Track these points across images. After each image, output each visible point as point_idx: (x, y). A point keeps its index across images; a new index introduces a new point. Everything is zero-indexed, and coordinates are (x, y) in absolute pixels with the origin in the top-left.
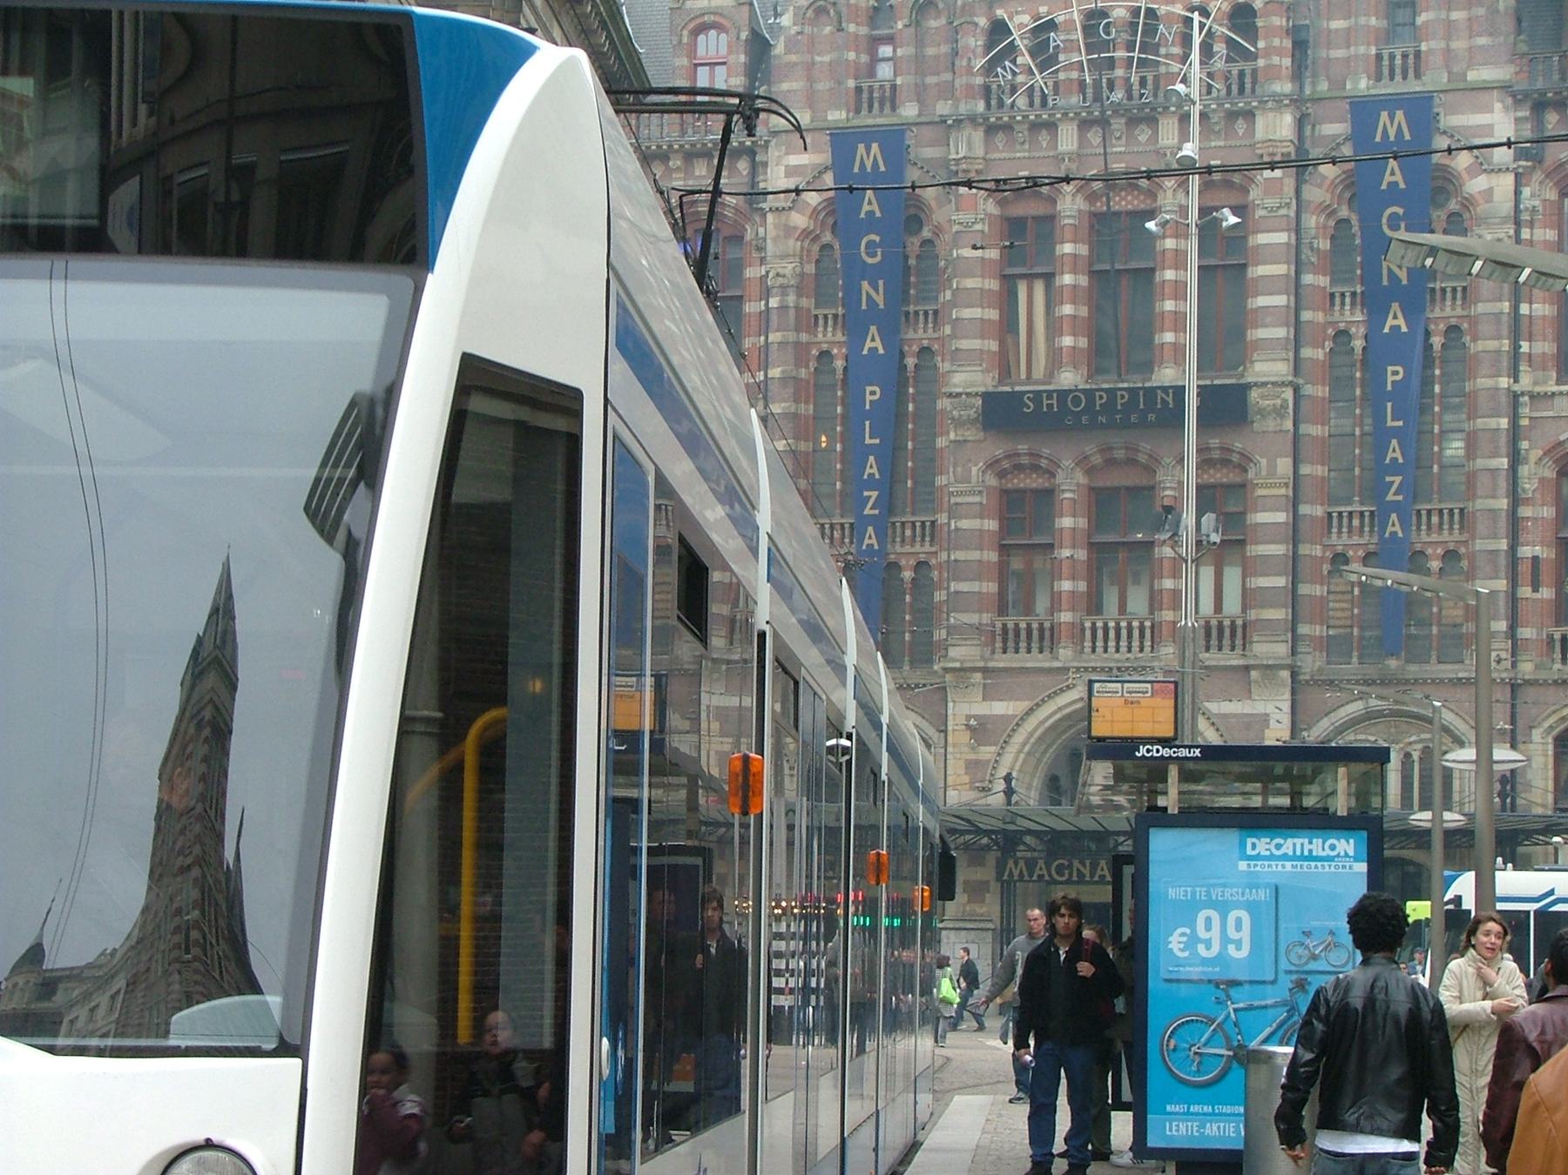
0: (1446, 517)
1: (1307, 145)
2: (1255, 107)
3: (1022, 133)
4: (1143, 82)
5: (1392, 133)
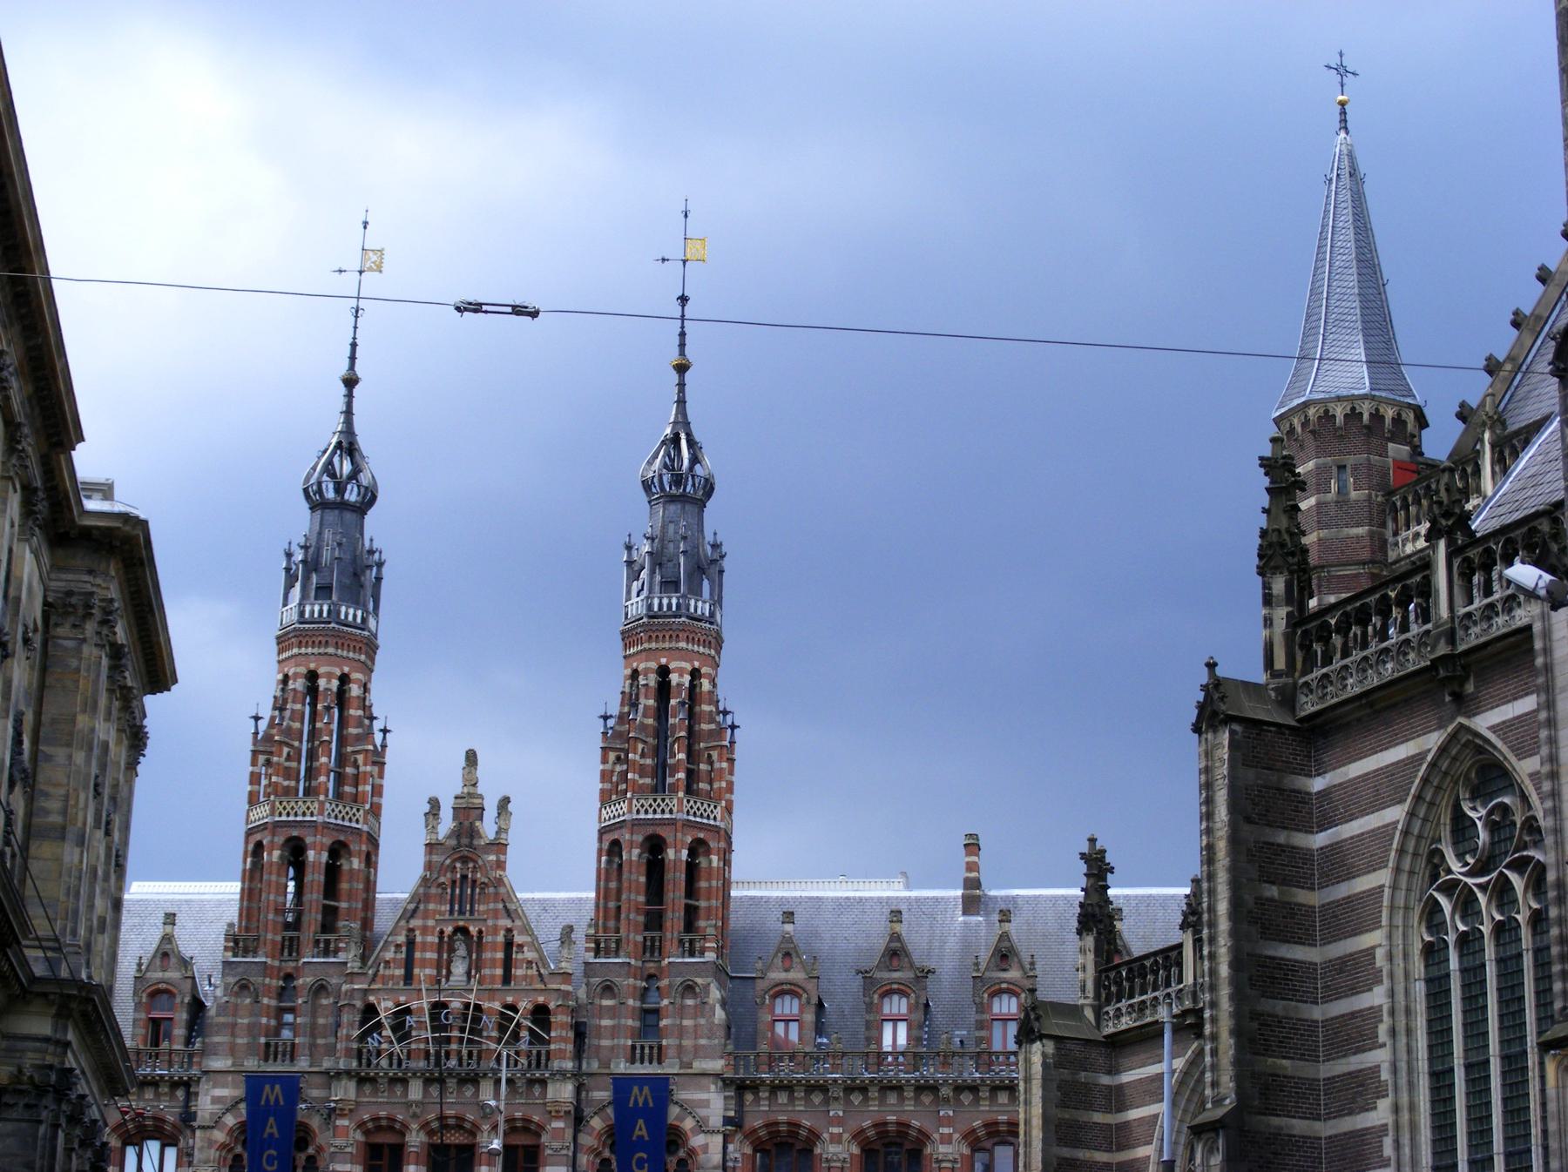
1: (583, 1105)
4: (470, 1054)
5: (641, 1101)
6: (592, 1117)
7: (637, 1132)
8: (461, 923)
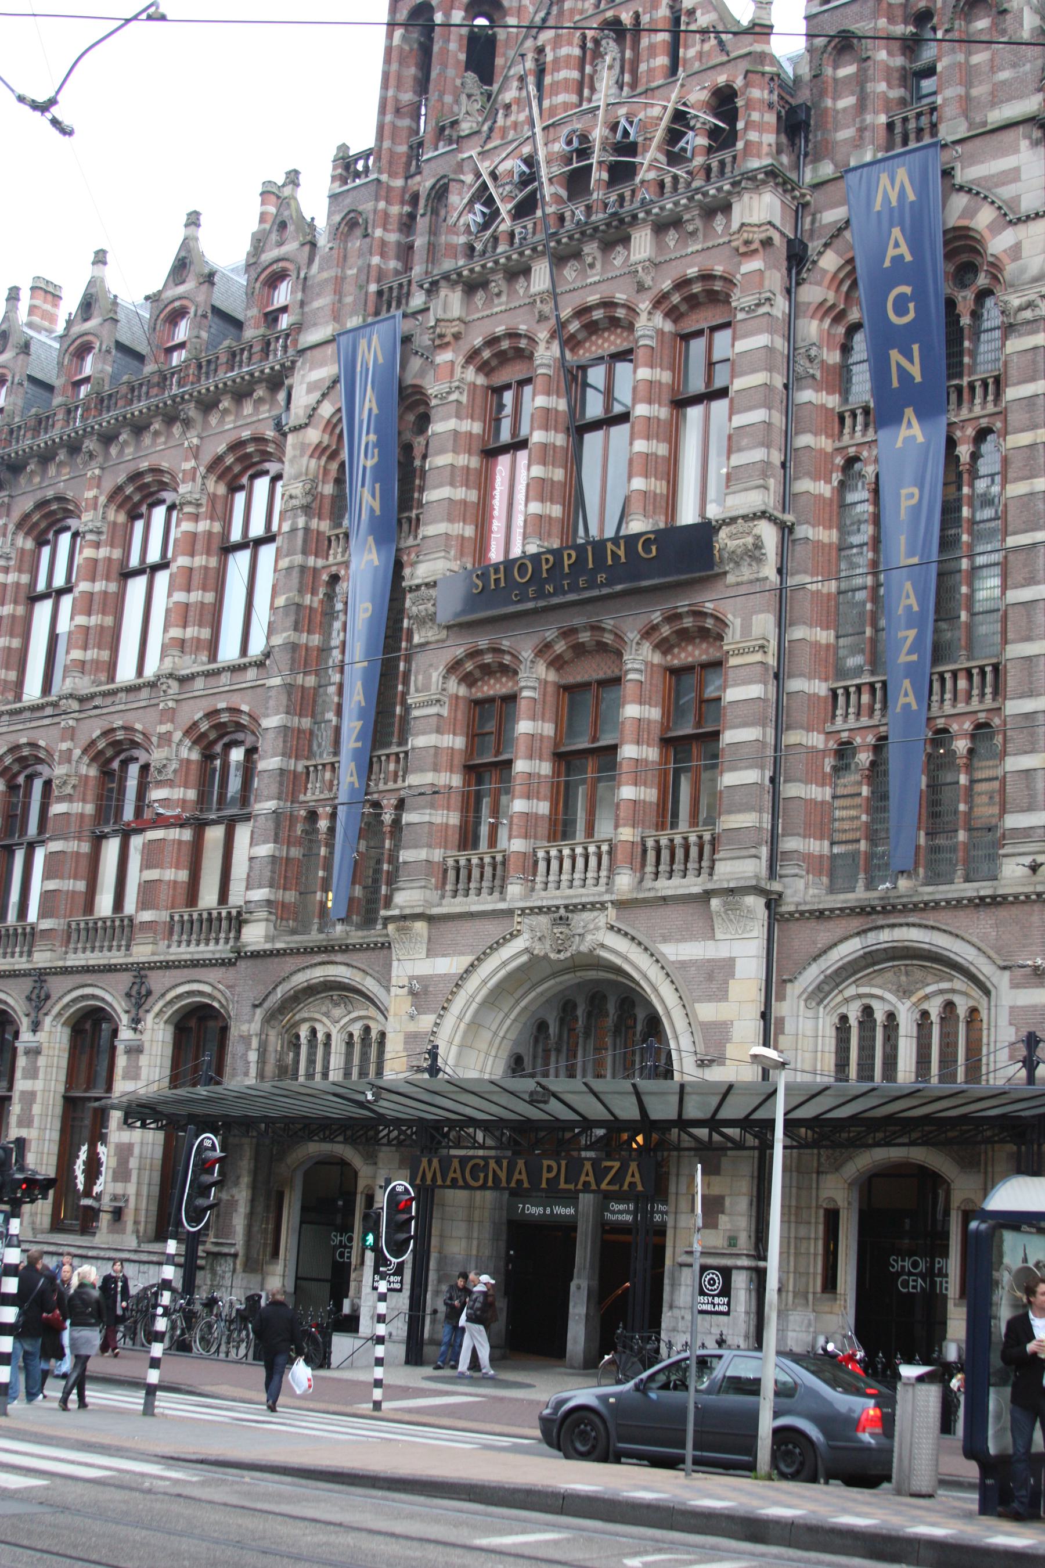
0: (976, 679)
2: (729, 193)
3: (499, 281)
6: (820, 254)
7: (891, 252)
8: (609, 14)
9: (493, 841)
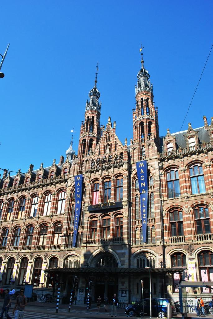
0: (152, 220)
7: (141, 172)
9: (94, 238)
